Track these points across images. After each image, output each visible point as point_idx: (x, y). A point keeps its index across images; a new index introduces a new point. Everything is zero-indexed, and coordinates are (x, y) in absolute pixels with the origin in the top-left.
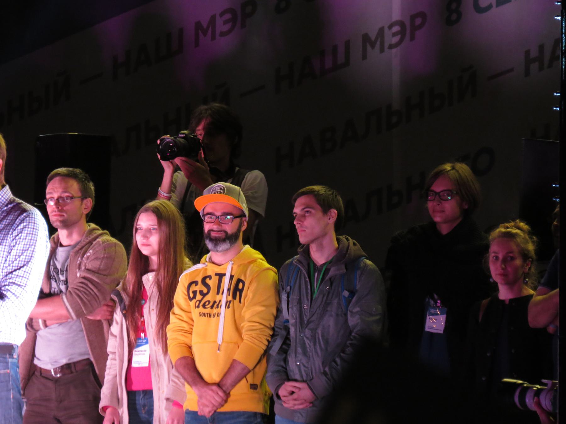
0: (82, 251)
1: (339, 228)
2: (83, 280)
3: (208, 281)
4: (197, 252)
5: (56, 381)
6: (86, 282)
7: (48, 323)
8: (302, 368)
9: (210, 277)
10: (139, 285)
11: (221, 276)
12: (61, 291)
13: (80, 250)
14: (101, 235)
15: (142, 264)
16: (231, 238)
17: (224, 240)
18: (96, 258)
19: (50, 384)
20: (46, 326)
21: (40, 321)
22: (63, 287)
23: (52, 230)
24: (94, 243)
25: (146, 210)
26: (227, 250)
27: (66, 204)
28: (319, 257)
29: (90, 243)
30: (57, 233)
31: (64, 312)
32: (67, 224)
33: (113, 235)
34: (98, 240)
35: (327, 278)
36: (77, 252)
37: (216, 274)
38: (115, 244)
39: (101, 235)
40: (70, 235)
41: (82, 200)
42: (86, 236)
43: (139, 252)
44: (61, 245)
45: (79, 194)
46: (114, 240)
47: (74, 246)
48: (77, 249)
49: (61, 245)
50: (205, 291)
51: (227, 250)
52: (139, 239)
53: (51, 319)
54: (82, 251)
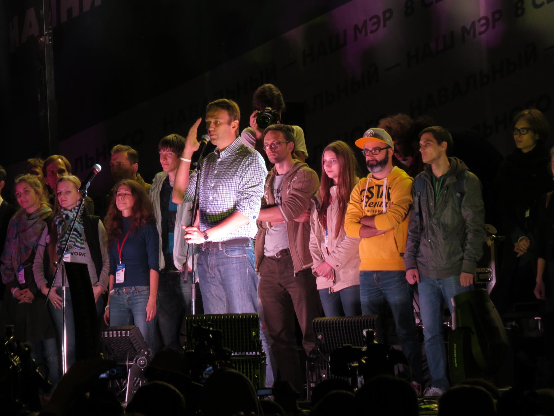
0: (290, 178)
1: (450, 153)
2: (292, 196)
3: (371, 190)
4: (364, 173)
5: (278, 260)
6: (294, 198)
7: (272, 224)
8: (432, 244)
9: (373, 187)
10: (328, 196)
11: (379, 186)
12: (278, 204)
13: (289, 176)
14: (302, 166)
15: (329, 183)
16: (383, 163)
17: (376, 166)
18: (300, 182)
19: (275, 263)
20: (271, 226)
21: (267, 223)
22: (279, 201)
23: (269, 165)
24: (298, 172)
25: (328, 149)
26: (381, 171)
27: (276, 148)
28: (439, 171)
29: (296, 172)
30: (274, 168)
31: (280, 217)
32: (279, 160)
33: (310, 167)
34: (301, 170)
35: (445, 185)
36: (287, 178)
37: (376, 185)
38: (311, 172)
39: (302, 166)
40: (281, 167)
41: (287, 143)
42: (293, 168)
43: (326, 176)
44: (278, 175)
45: (284, 140)
46: (310, 169)
47: (286, 174)
48: (288, 175)
49: (278, 175)
50: (370, 196)
51: (381, 171)
52: (325, 167)
53: (273, 222)
54: (290, 178)
